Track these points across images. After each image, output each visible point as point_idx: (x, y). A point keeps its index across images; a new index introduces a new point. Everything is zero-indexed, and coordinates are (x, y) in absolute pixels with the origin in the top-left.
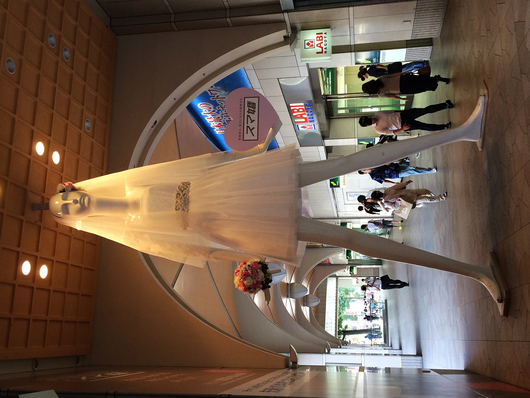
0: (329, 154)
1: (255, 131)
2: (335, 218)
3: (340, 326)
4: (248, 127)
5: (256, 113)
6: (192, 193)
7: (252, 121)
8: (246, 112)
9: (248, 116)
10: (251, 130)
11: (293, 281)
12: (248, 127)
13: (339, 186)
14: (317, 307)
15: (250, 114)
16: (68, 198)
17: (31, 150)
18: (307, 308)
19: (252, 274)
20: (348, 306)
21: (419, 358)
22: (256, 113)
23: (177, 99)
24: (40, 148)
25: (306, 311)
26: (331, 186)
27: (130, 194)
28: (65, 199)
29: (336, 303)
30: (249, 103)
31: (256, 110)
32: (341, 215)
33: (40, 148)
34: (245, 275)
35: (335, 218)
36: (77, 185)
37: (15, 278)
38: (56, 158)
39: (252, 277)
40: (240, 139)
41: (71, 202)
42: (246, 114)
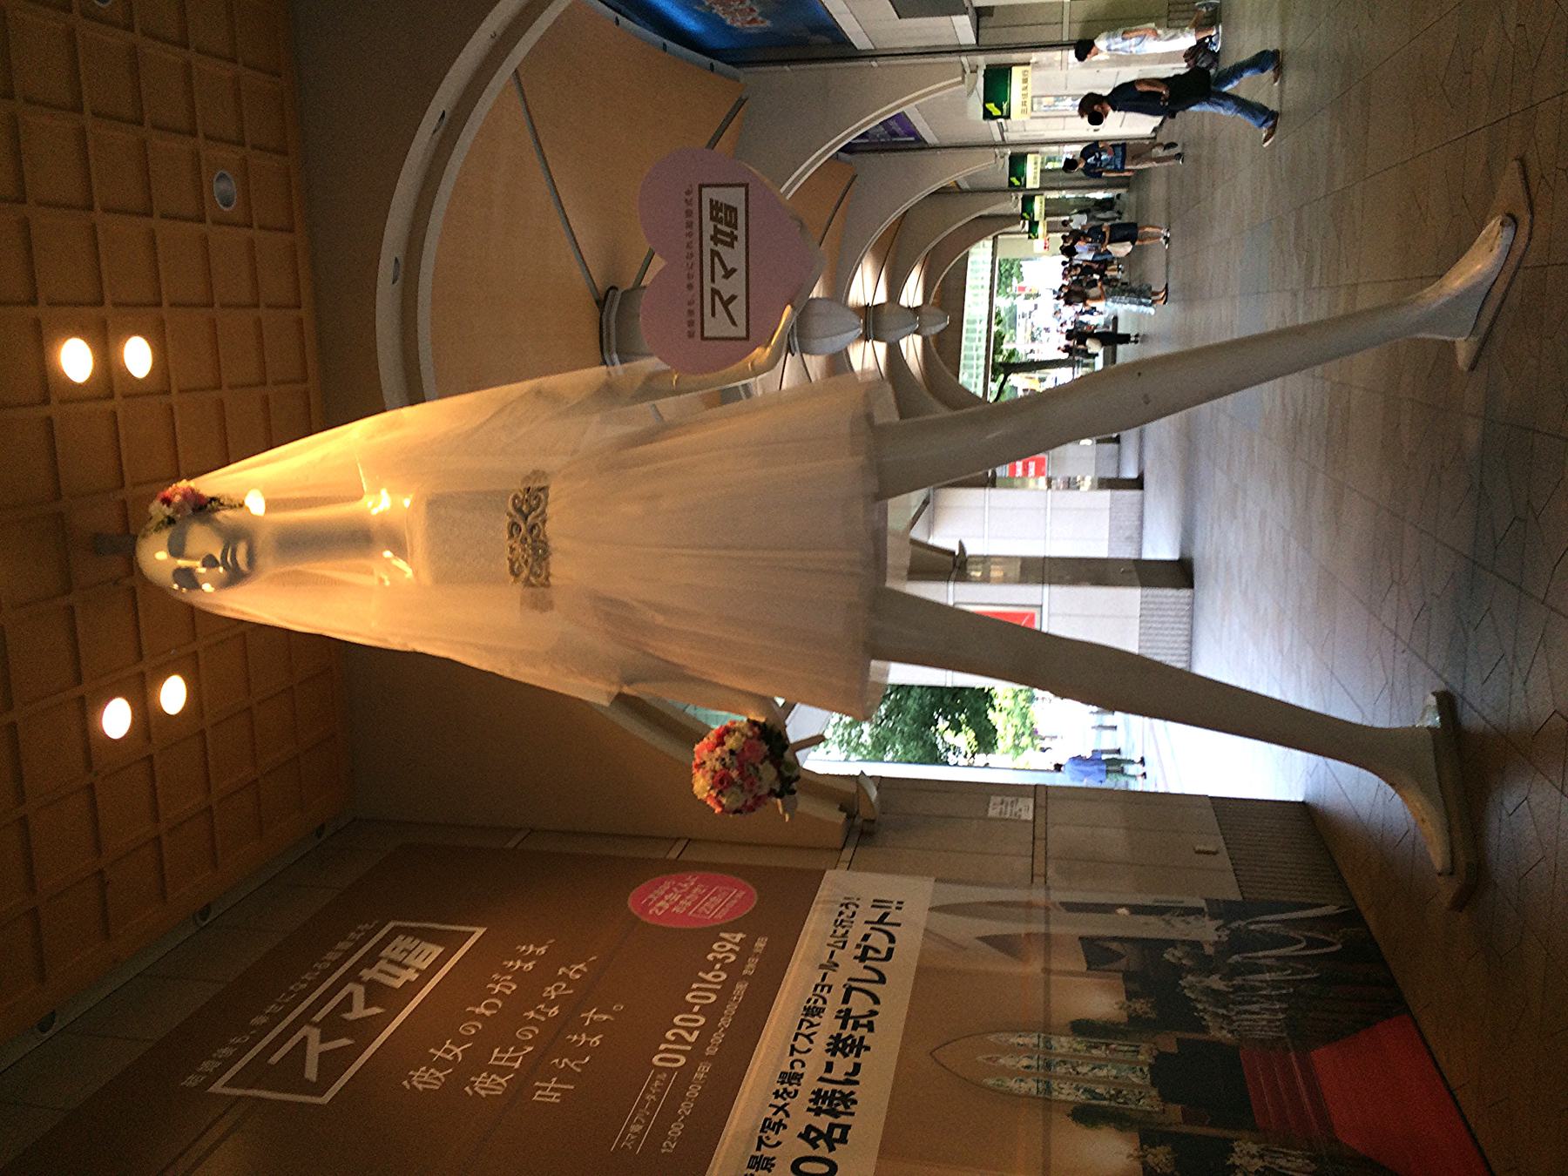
0: (984, 21)
1: (738, 308)
2: (995, 146)
3: (998, 351)
4: (715, 292)
5: (740, 245)
6: (558, 524)
7: (729, 273)
8: (706, 237)
9: (714, 253)
10: (726, 304)
11: (881, 297)
12: (715, 292)
13: (1008, 117)
14: (939, 337)
15: (720, 248)
16: (189, 550)
17: (49, 382)
18: (918, 339)
19: (743, 779)
20: (1020, 277)
21: (1185, 593)
22: (740, 245)
23: (499, 33)
24: (75, 360)
25: (912, 348)
26: (988, 115)
27: (380, 503)
28: (177, 551)
29: (993, 271)
30: (715, 206)
31: (740, 232)
32: (1011, 136)
33: (75, 360)
34: (721, 782)
35: (995, 146)
36: (211, 484)
37: (89, 765)
38: (138, 357)
39: (741, 786)
40: (691, 335)
41: (198, 563)
42: (708, 245)
